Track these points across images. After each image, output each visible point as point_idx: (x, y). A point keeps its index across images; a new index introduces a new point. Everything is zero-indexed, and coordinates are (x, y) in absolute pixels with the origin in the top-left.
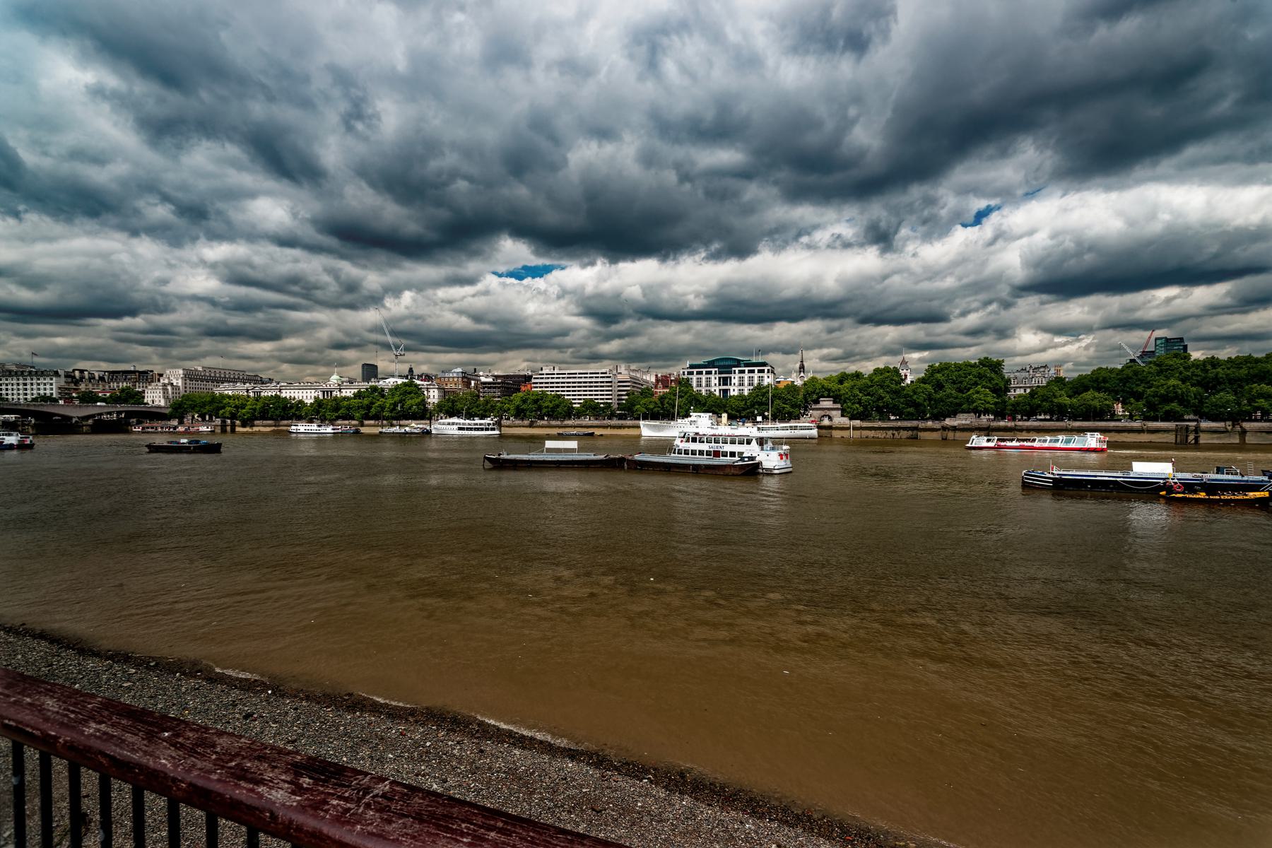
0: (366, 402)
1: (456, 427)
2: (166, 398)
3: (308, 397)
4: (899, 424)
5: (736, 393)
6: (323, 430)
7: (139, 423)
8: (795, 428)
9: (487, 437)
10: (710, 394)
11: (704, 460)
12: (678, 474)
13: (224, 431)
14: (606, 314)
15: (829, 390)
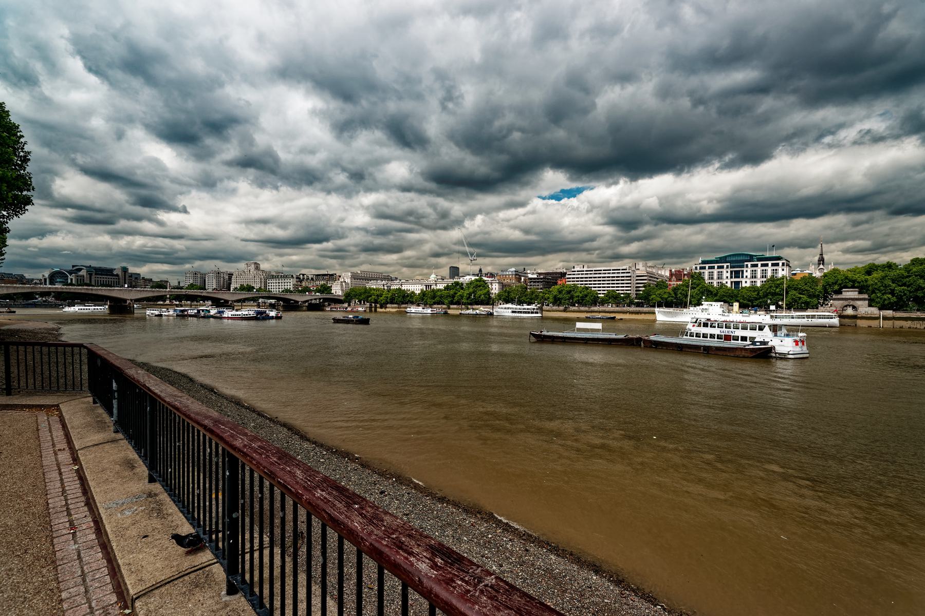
0: (452, 292)
2: (342, 290)
3: (417, 289)
5: (748, 285)
6: (425, 311)
7: (329, 305)
8: (813, 317)
9: (532, 318)
10: (722, 285)
11: (715, 343)
12: (687, 353)
13: (371, 311)
14: (627, 222)
15: (854, 281)
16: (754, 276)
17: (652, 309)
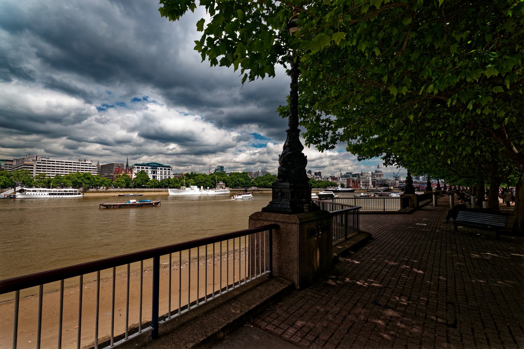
1: (46, 193)
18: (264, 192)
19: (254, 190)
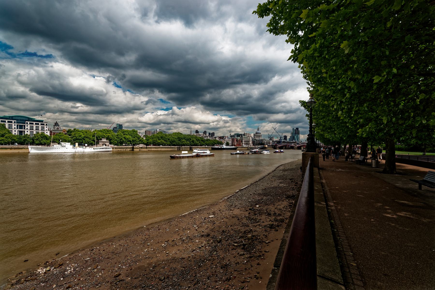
4: (126, 147)
16: (32, 128)
17: (26, 146)
18: (153, 149)
19: (142, 148)
